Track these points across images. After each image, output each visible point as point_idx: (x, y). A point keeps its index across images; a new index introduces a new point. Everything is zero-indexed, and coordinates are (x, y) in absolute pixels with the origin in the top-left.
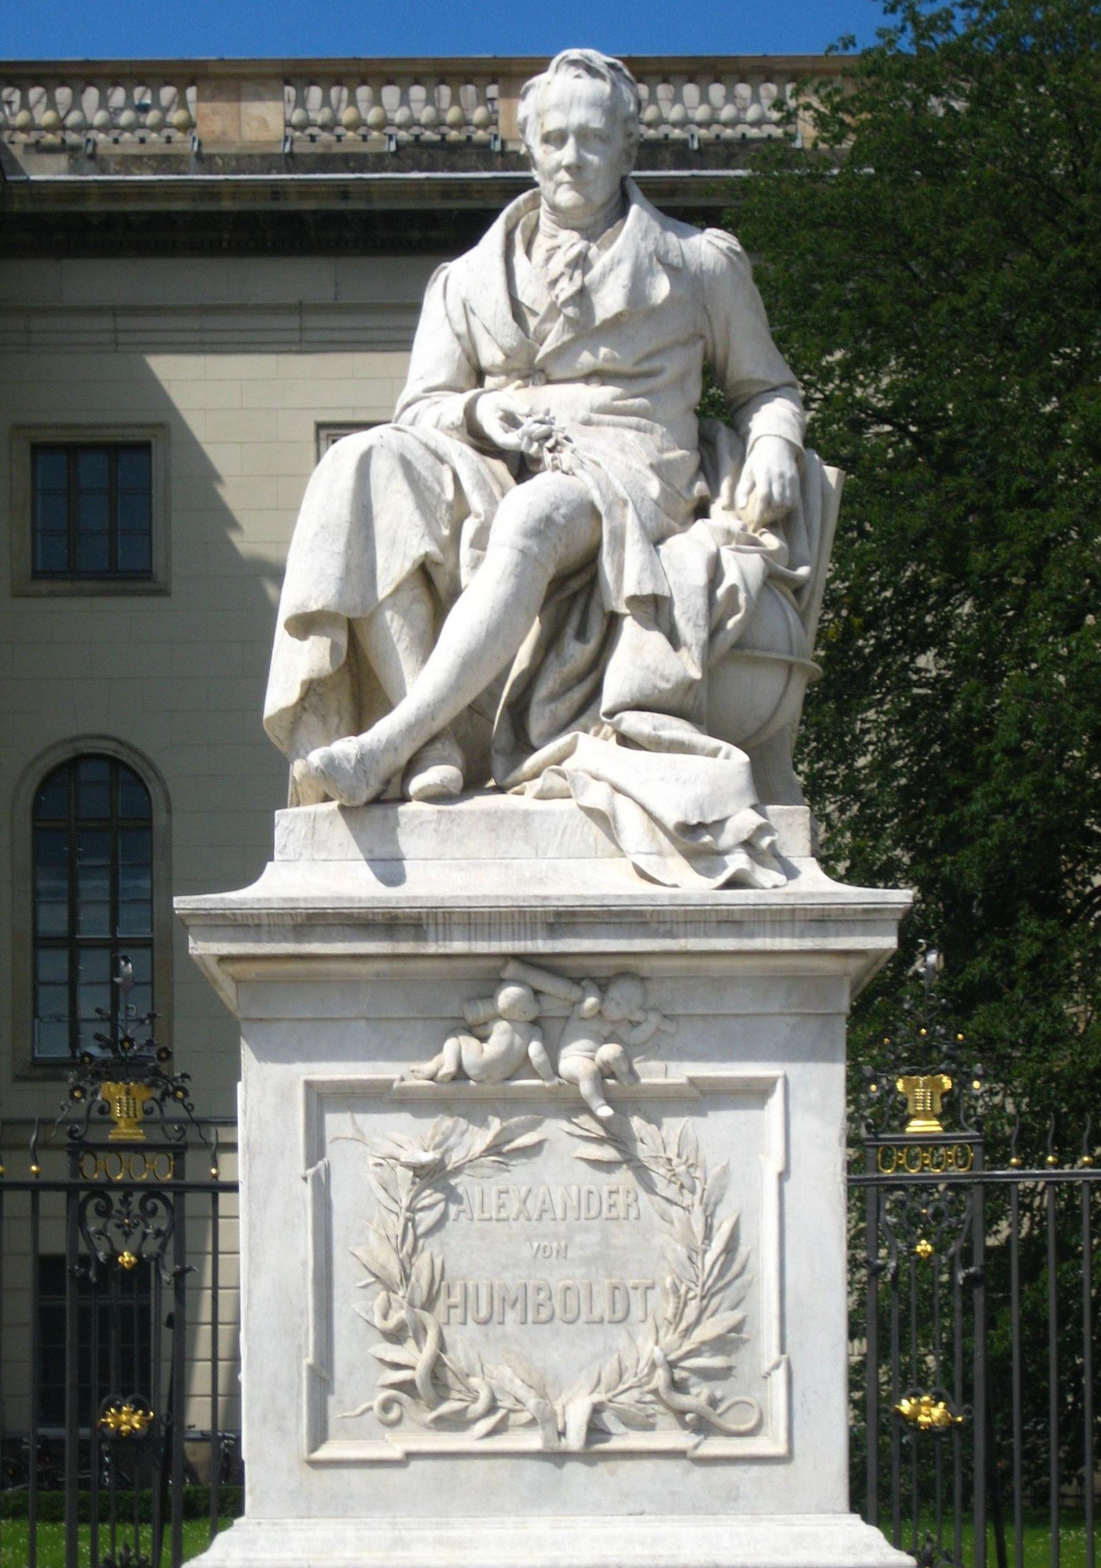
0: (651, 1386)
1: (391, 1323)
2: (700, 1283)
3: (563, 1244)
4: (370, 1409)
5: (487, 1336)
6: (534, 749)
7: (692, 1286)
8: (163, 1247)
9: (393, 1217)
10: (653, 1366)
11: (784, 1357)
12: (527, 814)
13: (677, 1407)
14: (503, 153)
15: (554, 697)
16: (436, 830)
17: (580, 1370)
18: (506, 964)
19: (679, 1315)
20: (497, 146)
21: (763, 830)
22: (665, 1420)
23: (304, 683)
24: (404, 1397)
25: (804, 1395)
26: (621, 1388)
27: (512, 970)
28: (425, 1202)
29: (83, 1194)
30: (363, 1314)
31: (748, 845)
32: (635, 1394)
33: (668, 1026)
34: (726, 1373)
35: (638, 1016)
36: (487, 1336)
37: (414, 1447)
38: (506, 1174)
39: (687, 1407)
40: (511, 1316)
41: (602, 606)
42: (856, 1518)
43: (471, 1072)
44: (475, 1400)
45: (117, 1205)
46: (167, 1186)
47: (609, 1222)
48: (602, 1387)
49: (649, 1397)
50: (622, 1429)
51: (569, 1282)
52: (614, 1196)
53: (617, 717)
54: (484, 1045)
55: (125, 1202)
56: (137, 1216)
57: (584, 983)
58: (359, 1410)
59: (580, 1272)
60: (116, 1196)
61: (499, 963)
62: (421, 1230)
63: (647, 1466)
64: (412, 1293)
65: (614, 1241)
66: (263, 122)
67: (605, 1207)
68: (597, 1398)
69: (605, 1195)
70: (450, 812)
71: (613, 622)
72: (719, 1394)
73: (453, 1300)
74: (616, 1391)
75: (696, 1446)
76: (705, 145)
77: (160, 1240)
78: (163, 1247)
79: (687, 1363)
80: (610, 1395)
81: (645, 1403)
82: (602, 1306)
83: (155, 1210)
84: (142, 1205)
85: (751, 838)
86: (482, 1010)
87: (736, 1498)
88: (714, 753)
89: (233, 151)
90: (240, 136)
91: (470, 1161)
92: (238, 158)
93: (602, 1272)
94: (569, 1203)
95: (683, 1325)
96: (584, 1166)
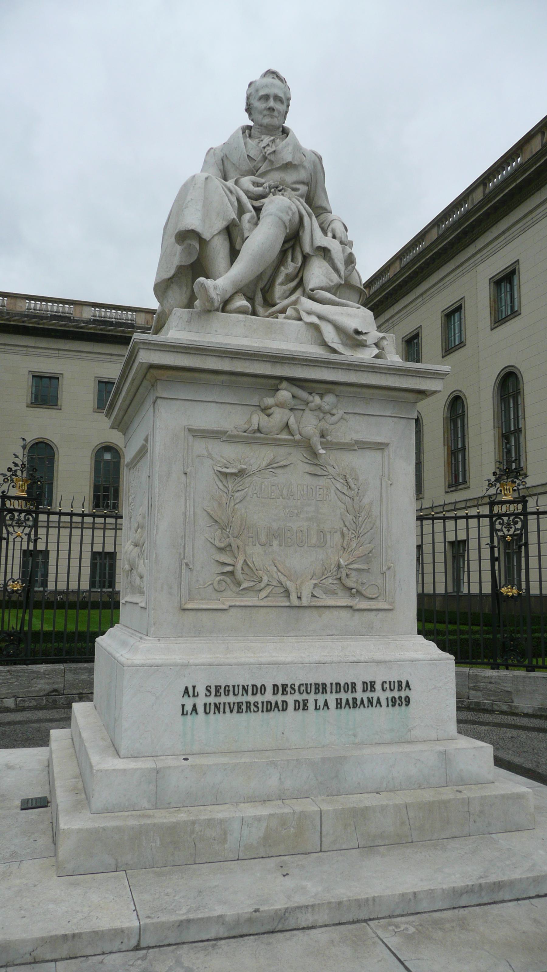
0: (338, 576)
1: (222, 545)
2: (357, 531)
3: (299, 511)
4: (212, 584)
5: (265, 551)
6: (274, 305)
7: (354, 532)
8: (31, 531)
9: (225, 495)
10: (339, 567)
11: (392, 565)
12: (282, 323)
13: (348, 586)
14: (74, 319)
15: (282, 284)
16: (244, 325)
17: (305, 569)
18: (281, 382)
19: (348, 545)
20: (72, 318)
21: (384, 338)
22: (340, 593)
23: (177, 266)
24: (228, 580)
25: (400, 582)
26: (324, 577)
27: (285, 384)
28: (240, 488)
29: (5, 513)
30: (210, 539)
31: (376, 344)
32: (330, 580)
33: (346, 416)
34: (367, 571)
35: (334, 411)
36: (265, 551)
37: (233, 604)
38: (275, 478)
39: (352, 587)
40: (275, 543)
41: (302, 252)
42: (421, 637)
43: (263, 430)
44: (261, 581)
45: (16, 517)
46: (33, 512)
47: (319, 502)
48: (314, 577)
49: (335, 582)
50: (324, 596)
51: (302, 529)
52: (321, 490)
53: (315, 291)
54: (269, 418)
55: (19, 516)
56: (23, 520)
57: (313, 394)
58: (206, 585)
59: (306, 524)
60: (16, 514)
61: (277, 382)
62: (238, 501)
63: (335, 612)
64: (233, 530)
65: (321, 511)
66: (21, 307)
67: (317, 495)
68: (314, 582)
69: (317, 489)
70: (251, 318)
71: (306, 258)
72: (365, 581)
73: (250, 535)
74: (322, 579)
75: (356, 604)
76: (116, 323)
77: (30, 529)
78: (31, 531)
79: (351, 567)
80: (319, 580)
81: (333, 584)
82: (314, 541)
83: (29, 518)
84: (25, 517)
85: (377, 343)
86: (270, 401)
87: (372, 628)
88: (359, 308)
89: (14, 312)
90: (16, 309)
91: (260, 471)
92: (15, 313)
93: (315, 524)
94: (302, 492)
95: (350, 550)
96: (308, 476)
